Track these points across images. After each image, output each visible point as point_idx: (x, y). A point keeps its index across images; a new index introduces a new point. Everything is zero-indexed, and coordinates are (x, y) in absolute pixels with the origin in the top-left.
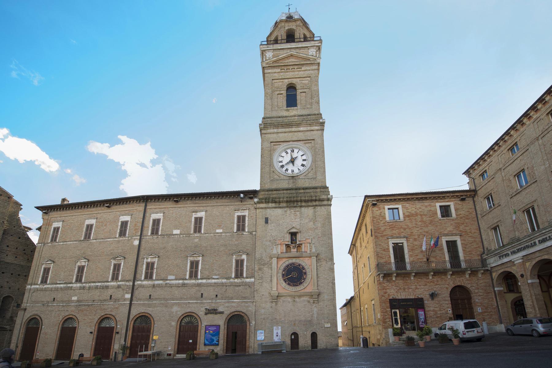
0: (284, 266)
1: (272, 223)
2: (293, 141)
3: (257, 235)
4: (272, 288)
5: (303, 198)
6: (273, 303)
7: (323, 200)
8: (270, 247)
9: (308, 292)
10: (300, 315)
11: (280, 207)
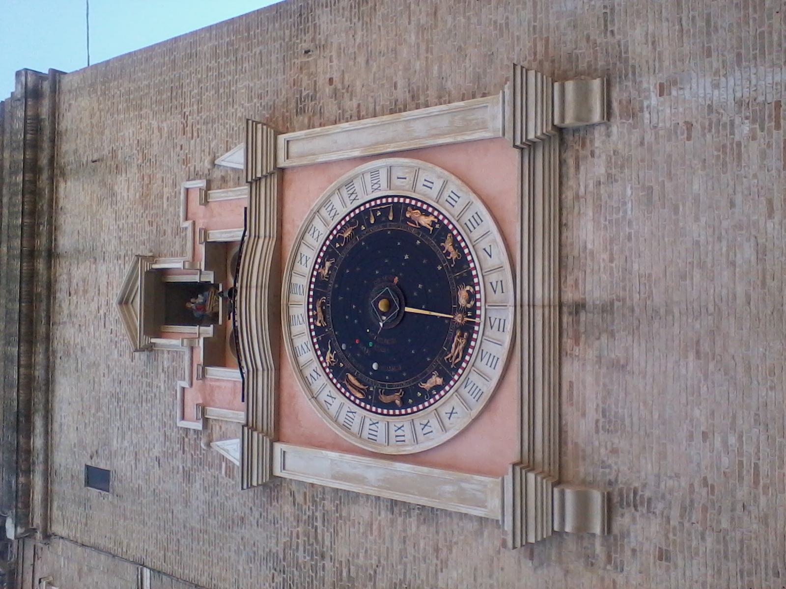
1: (106, 444)
3: (158, 565)
4: (481, 520)
5: (17, 243)
6: (625, 535)
7: (34, 125)
8: (217, 482)
9: (528, 176)
10: (761, 253)
11: (49, 383)
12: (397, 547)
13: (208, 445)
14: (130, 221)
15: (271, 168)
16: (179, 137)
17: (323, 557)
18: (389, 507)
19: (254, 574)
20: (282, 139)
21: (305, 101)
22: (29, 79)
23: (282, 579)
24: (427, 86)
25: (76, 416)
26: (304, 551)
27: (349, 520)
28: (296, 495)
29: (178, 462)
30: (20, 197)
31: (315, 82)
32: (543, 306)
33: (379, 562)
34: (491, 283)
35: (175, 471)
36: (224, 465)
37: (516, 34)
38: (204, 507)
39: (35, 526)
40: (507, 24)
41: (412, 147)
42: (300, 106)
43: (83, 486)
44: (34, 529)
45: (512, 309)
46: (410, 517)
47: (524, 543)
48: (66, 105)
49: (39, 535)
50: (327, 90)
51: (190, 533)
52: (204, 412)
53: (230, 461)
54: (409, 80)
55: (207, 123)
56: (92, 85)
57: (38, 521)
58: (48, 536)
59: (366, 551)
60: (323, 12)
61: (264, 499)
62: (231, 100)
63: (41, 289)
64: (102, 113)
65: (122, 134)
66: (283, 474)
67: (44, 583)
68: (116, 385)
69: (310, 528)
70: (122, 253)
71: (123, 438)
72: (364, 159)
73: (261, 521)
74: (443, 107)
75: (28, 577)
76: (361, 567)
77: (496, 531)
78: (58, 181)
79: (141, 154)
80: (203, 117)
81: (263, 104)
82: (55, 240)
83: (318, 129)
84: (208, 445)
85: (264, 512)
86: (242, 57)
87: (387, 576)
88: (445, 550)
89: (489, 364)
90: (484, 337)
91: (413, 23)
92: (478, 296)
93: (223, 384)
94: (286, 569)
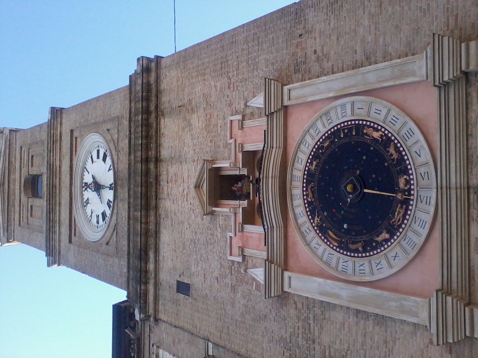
0: (317, 240)
1: (189, 268)
2: (71, 185)
3: (217, 340)
4: (415, 325)
11: (157, 233)
12: (360, 339)
13: (245, 271)
14: (200, 140)
15: (279, 106)
16: (226, 91)
17: (314, 342)
18: (355, 314)
19: (273, 350)
20: (286, 88)
21: (299, 64)
22: (144, 61)
23: (289, 354)
24: (376, 51)
25: (172, 252)
26: (303, 339)
27: (330, 321)
28: (297, 303)
29: (228, 281)
30: (140, 128)
31: (306, 53)
32: (456, 188)
33: (349, 347)
34: (421, 173)
35: (227, 286)
36: (254, 283)
37: (435, 14)
38: (243, 308)
39: (150, 314)
40: (428, 8)
41: (367, 89)
42: (296, 68)
43: (175, 292)
44: (150, 315)
45: (435, 190)
46: (368, 321)
47: (445, 343)
48: (164, 75)
49: (152, 319)
50: (313, 58)
51: (235, 323)
52: (243, 251)
53: (258, 281)
54: (364, 48)
55: (242, 82)
56: (178, 63)
57: (151, 311)
58: (156, 320)
59: (341, 340)
60: (310, 11)
61: (278, 305)
62: (256, 67)
63: (152, 180)
64: (183, 79)
65: (195, 90)
66: (289, 291)
67: (155, 347)
68: (194, 234)
69: (306, 324)
70: (196, 159)
71: (198, 265)
72: (336, 98)
73: (276, 318)
74: (387, 63)
75: (147, 342)
76: (338, 350)
77: (425, 332)
78: (160, 119)
79: (205, 102)
80: (240, 78)
81: (274, 69)
82: (159, 151)
83: (307, 81)
84: (245, 271)
85: (278, 313)
86: (262, 41)
87: (354, 356)
88: (391, 343)
89: (420, 225)
90: (416, 209)
91: (366, 13)
92: (412, 182)
93: (253, 235)
94: (292, 348)
